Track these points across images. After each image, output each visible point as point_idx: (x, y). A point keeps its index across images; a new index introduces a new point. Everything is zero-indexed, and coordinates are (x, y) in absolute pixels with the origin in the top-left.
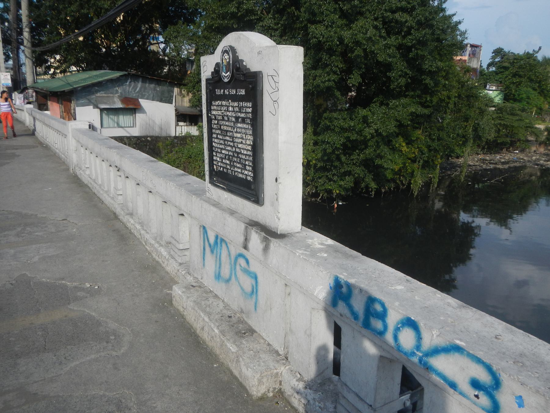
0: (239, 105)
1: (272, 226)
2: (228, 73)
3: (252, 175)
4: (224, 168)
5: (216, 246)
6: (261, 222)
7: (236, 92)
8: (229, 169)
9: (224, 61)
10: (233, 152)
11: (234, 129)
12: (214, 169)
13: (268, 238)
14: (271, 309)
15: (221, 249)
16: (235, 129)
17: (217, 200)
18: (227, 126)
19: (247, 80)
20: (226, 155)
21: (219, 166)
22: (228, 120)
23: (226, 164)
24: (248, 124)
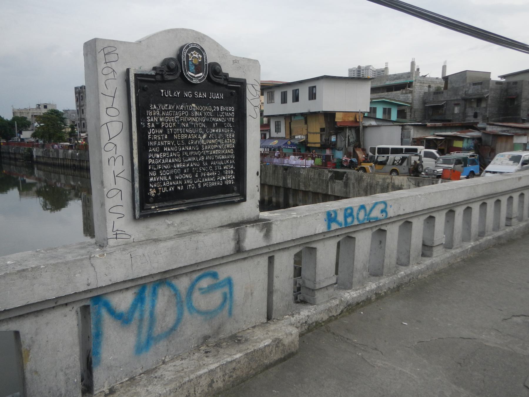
0: (212, 110)
1: (252, 217)
2: (201, 74)
3: (234, 177)
4: (176, 186)
5: (139, 305)
6: (237, 222)
7: (208, 95)
8: (190, 184)
9: (190, 59)
10: (201, 162)
11: (202, 135)
12: (150, 196)
13: (269, 223)
14: (252, 294)
15: (153, 301)
16: (204, 136)
17: (143, 239)
18: (188, 134)
19: (229, 85)
20: (182, 169)
21: (164, 187)
22: (191, 126)
23: (183, 180)
24: (227, 128)
